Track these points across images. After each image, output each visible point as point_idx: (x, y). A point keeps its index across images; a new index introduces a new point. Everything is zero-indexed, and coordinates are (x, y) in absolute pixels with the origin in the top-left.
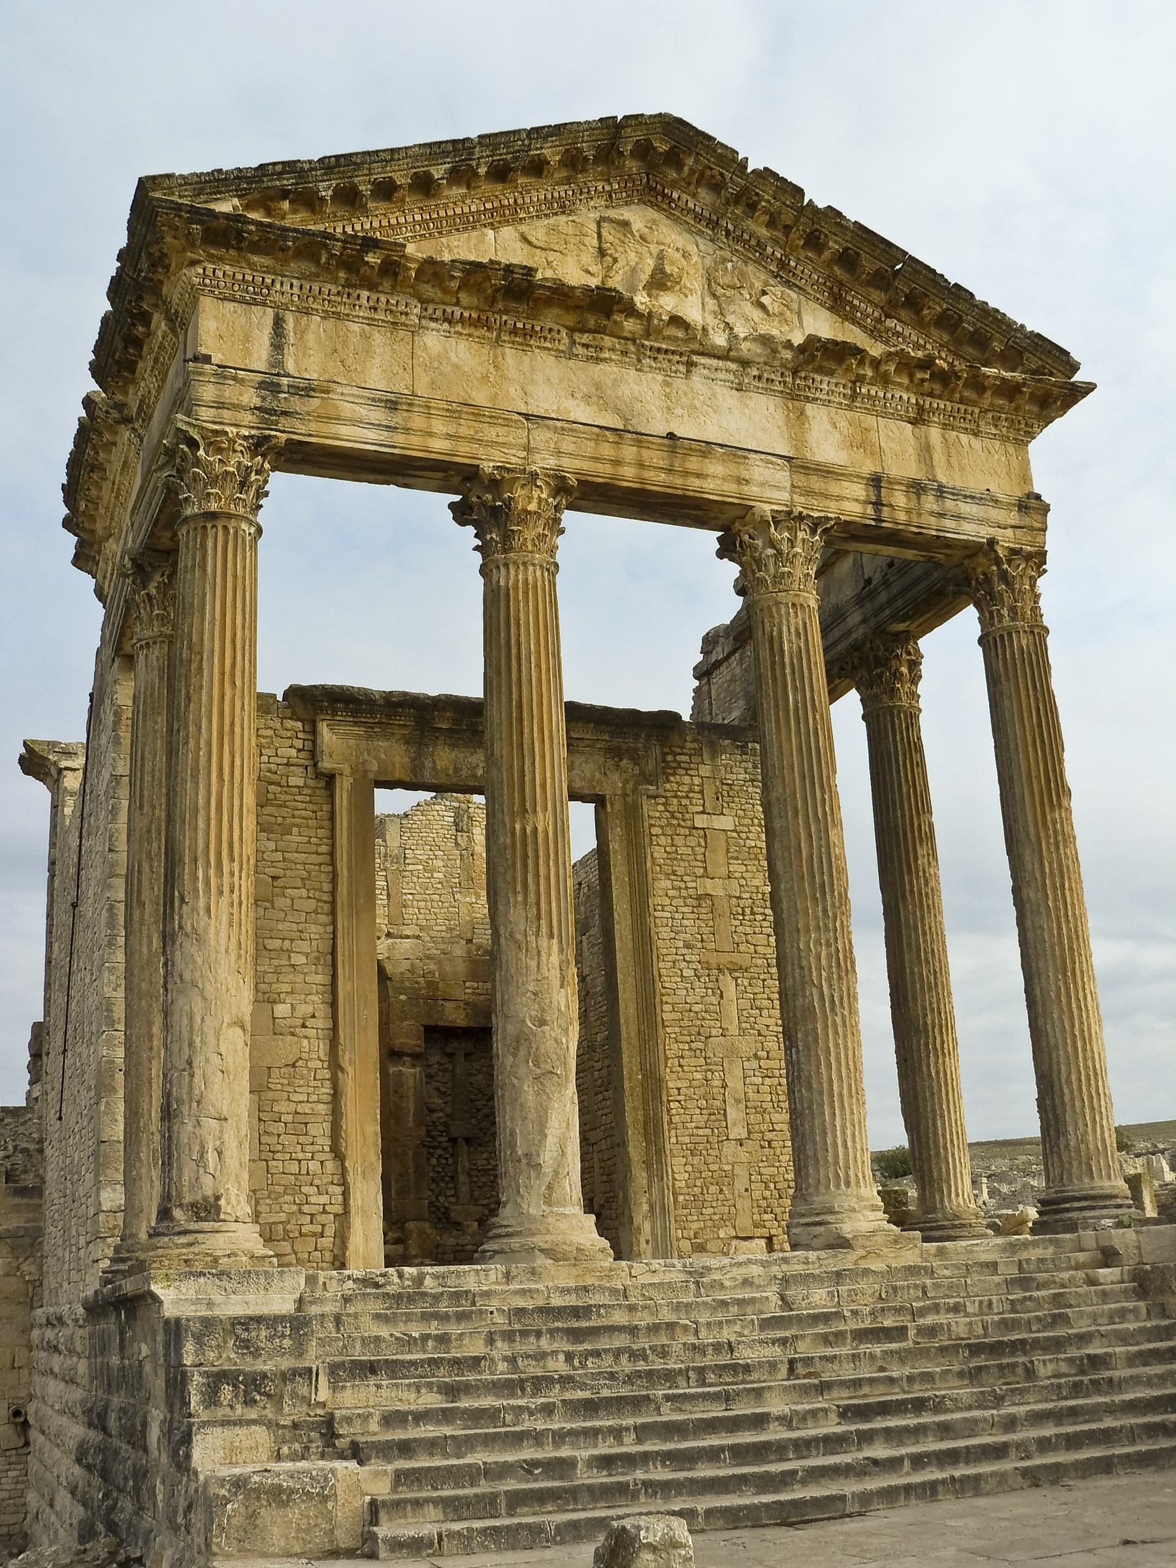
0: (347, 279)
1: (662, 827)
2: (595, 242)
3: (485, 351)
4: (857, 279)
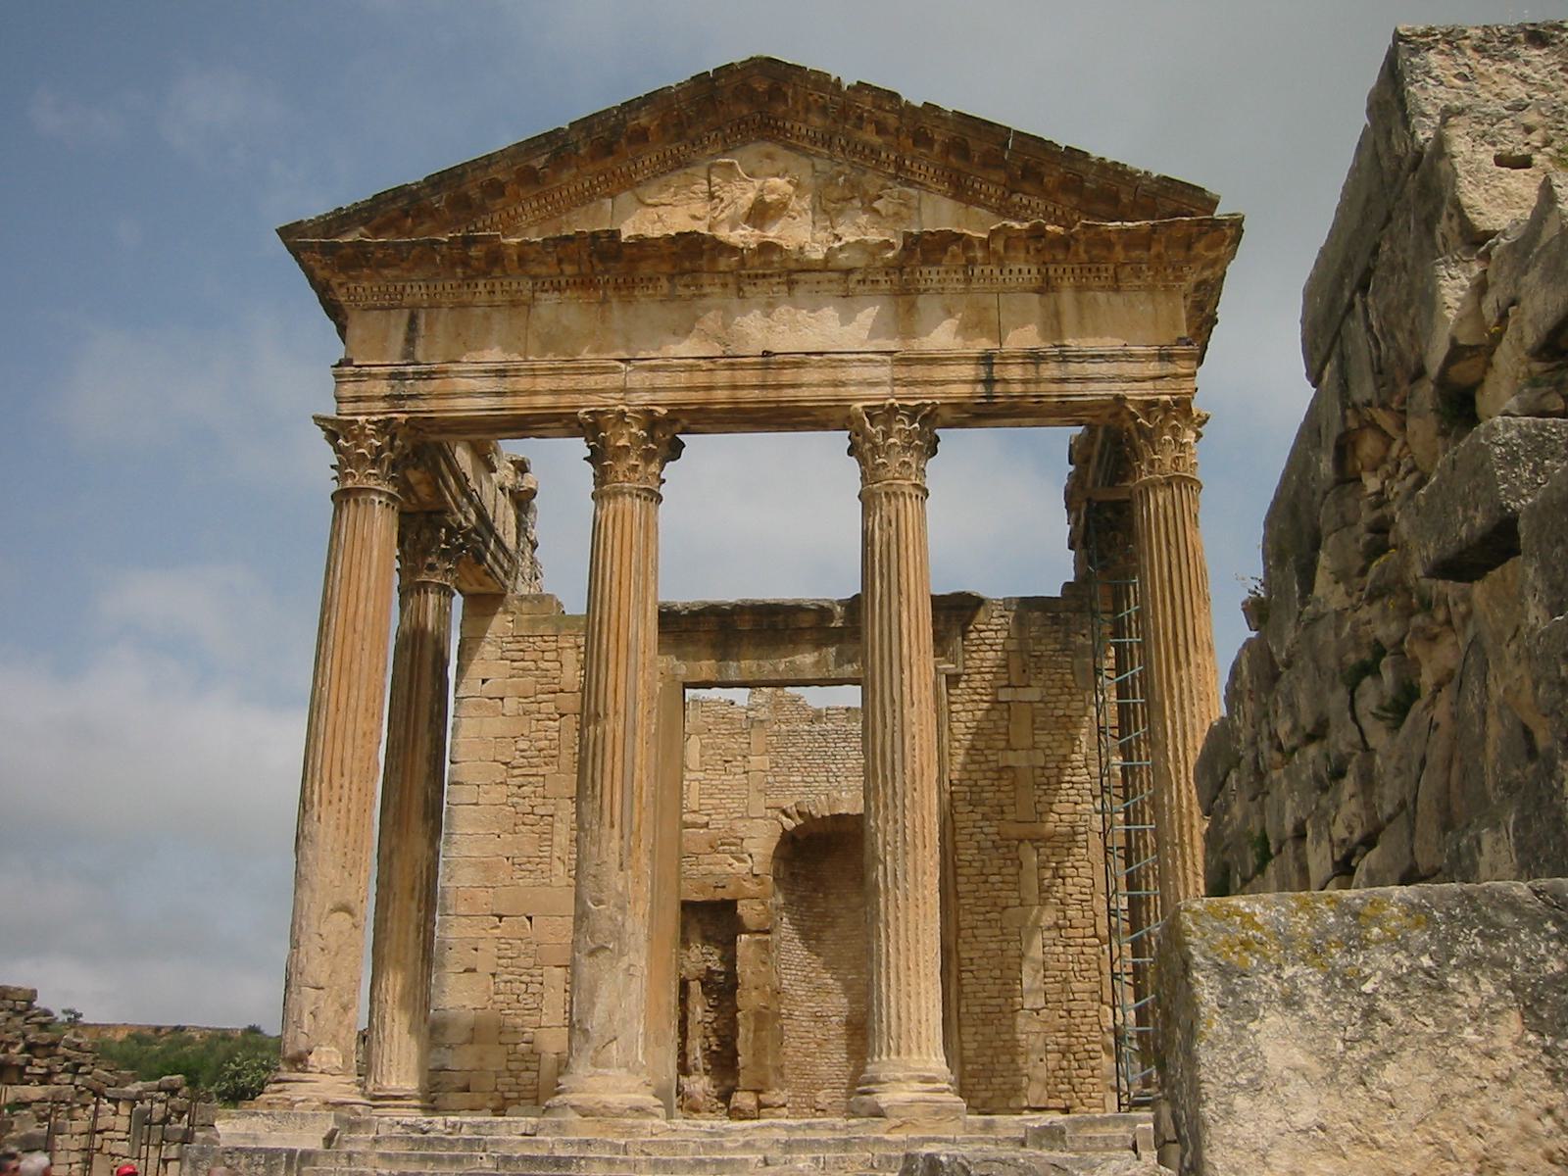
0: (464, 273)
1: (963, 703)
2: (705, 188)
3: (594, 308)
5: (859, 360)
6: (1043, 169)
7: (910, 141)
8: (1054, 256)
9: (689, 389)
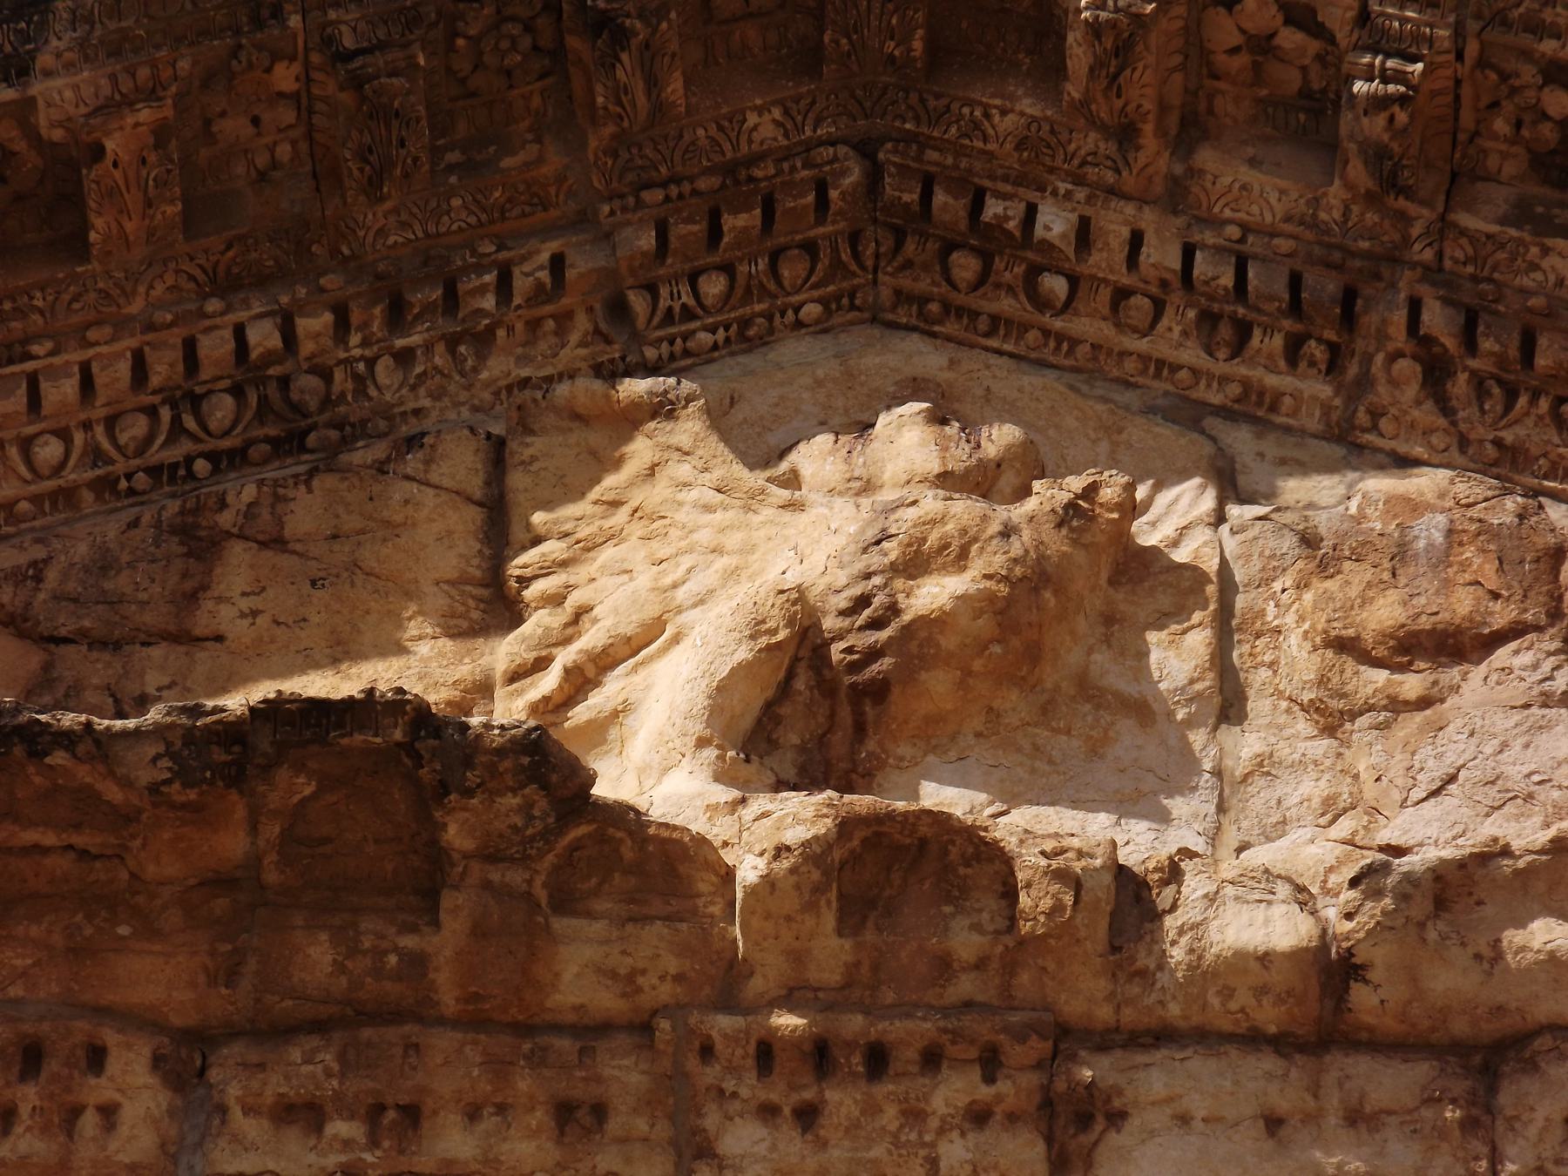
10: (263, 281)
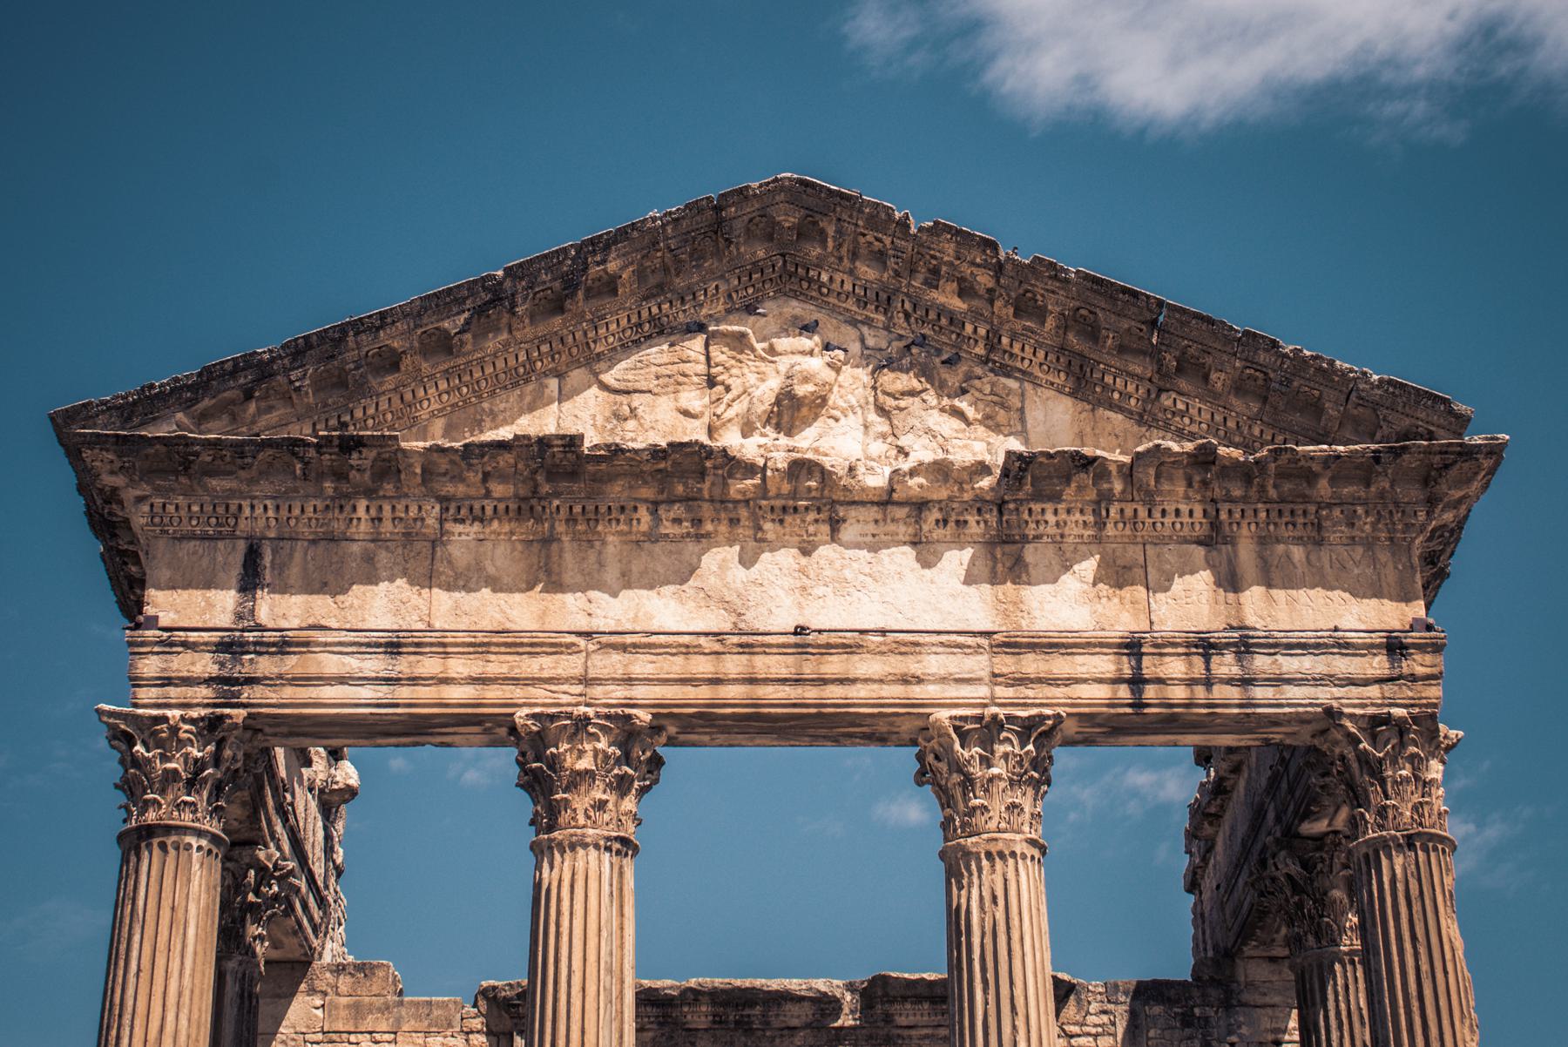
0: (336, 489)
2: (701, 368)
4: (1103, 347)
5: (942, 644)
6: (1209, 360)
7: (1011, 311)
8: (1228, 491)
9: (683, 681)
10: (654, 296)
